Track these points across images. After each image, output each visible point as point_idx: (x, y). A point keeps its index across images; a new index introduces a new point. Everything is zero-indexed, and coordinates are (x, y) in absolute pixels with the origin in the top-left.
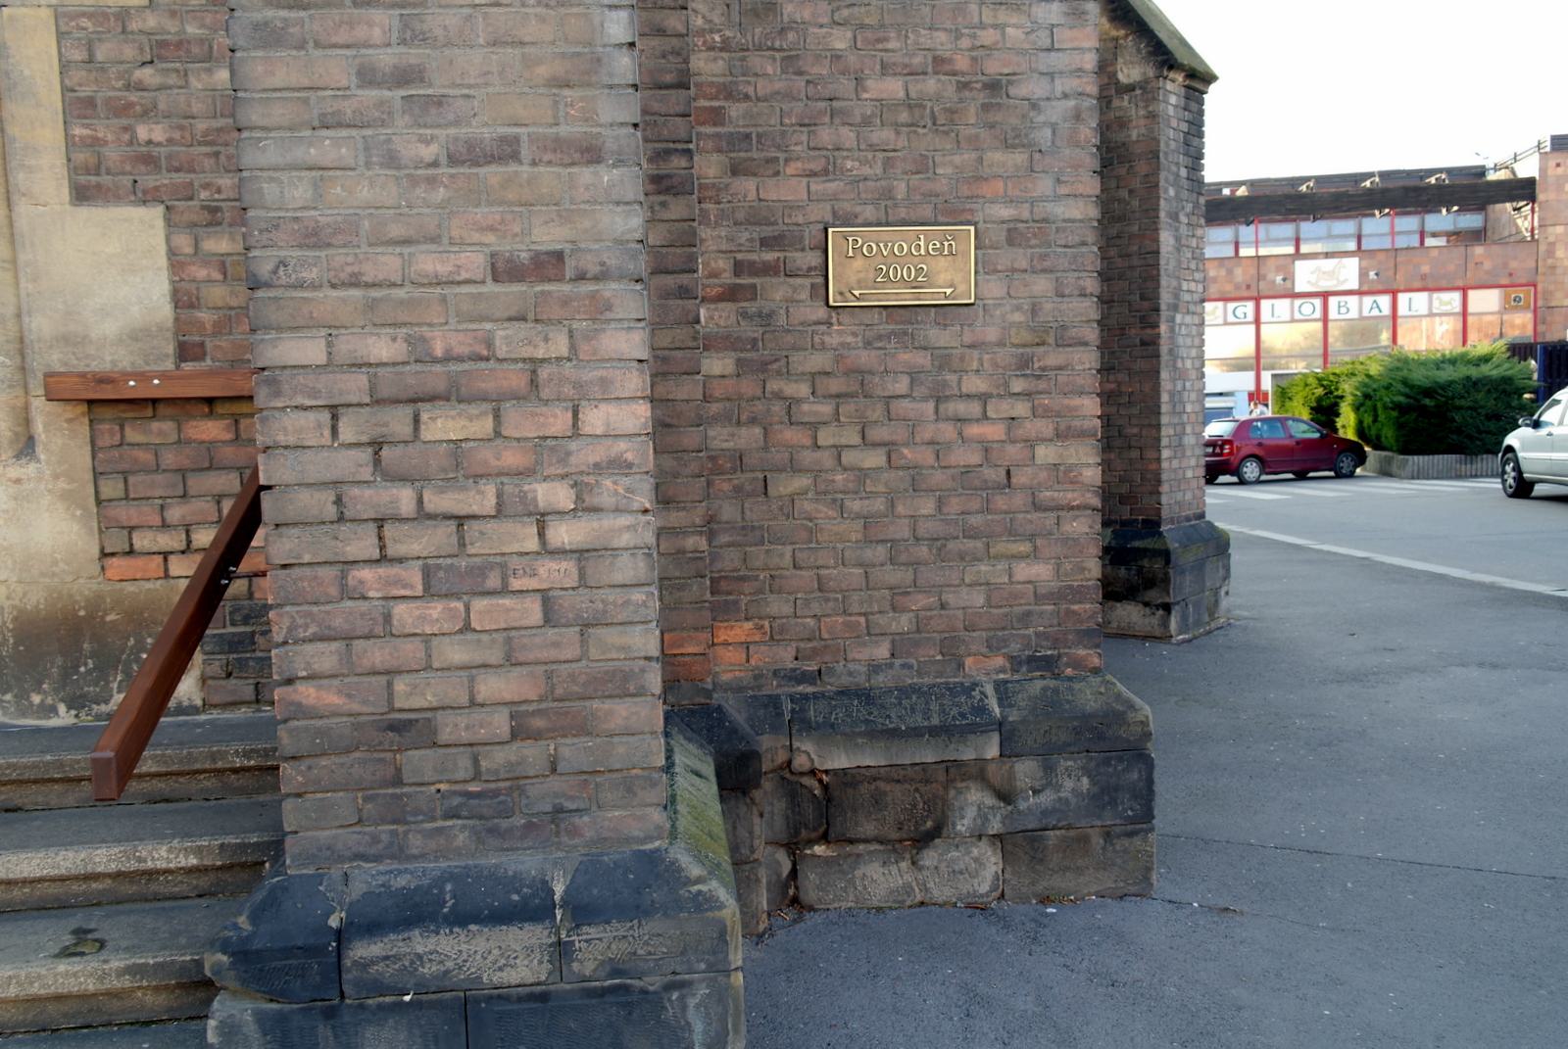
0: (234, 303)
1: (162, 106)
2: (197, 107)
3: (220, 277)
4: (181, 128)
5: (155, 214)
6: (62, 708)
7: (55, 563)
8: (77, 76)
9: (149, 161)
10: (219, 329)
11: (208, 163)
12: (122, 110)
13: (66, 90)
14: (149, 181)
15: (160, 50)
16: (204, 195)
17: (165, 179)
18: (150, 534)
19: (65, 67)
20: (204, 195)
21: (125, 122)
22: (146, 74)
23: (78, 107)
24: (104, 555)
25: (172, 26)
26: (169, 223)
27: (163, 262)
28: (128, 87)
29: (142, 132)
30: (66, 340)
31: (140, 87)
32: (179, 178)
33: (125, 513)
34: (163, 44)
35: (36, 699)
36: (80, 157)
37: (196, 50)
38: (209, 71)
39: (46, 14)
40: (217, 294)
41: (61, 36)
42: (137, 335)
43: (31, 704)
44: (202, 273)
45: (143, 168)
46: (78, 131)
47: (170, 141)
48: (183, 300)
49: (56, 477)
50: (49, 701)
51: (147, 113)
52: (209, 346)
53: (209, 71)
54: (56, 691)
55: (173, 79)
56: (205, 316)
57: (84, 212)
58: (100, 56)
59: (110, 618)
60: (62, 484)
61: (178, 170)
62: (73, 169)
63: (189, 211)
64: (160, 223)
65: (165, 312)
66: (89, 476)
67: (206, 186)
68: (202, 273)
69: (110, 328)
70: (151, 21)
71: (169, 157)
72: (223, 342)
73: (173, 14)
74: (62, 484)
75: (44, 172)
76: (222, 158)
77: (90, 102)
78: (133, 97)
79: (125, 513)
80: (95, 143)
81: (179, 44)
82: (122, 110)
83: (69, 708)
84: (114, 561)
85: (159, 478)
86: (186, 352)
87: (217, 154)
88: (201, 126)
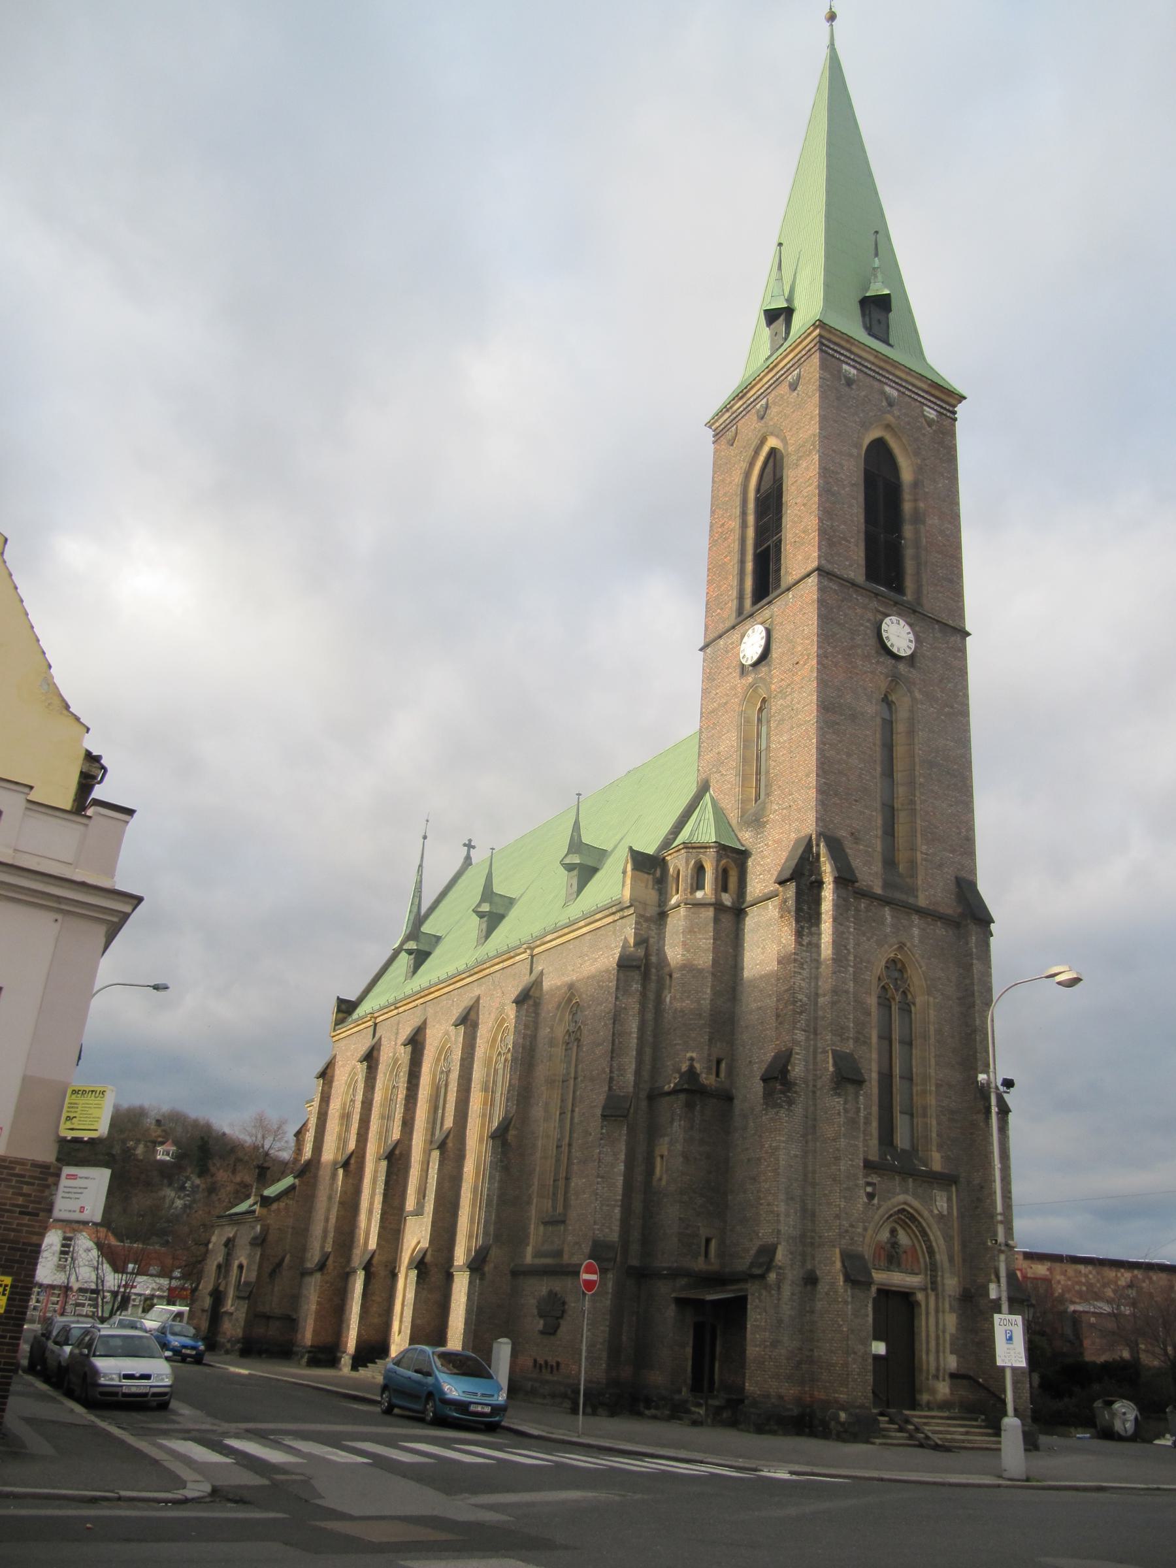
75: (948, 1350)
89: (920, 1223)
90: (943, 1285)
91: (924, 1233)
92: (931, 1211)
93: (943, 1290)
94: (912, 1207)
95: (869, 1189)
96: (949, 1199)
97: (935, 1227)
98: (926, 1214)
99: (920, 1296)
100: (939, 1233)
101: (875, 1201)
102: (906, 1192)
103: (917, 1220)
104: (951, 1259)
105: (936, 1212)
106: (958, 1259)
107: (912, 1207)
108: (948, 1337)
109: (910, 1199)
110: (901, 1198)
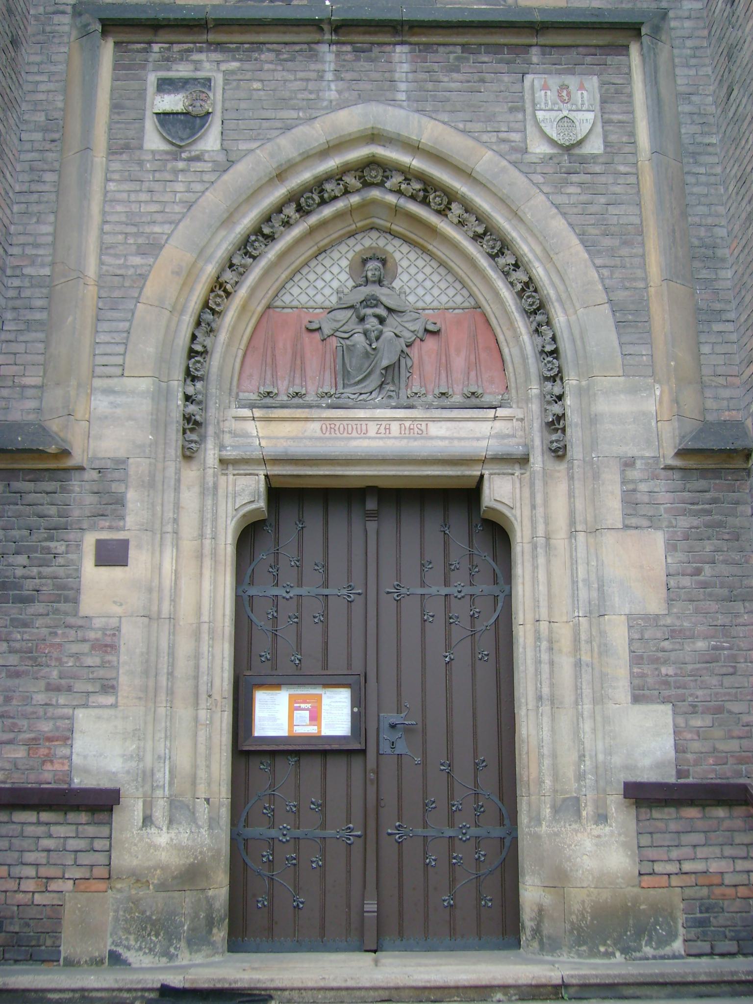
0: (703, 750)
1: (672, 658)
2: (688, 659)
3: (696, 737)
4: (681, 668)
5: (668, 708)
6: (618, 954)
7: (618, 877)
8: (636, 645)
9: (667, 683)
10: (697, 763)
11: (692, 684)
12: (655, 661)
13: (631, 651)
14: (666, 693)
15: (674, 634)
16: (690, 699)
17: (673, 692)
18: (662, 864)
19: (631, 640)
20: (690, 699)
21: (656, 666)
22: (666, 644)
23: (636, 659)
24: (640, 874)
25: (678, 623)
26: (675, 713)
27: (672, 731)
28: (657, 651)
29: (664, 670)
30: (627, 768)
31: (664, 650)
32: (680, 691)
33: (651, 853)
34: (673, 631)
35: (602, 949)
36: (636, 682)
37: (688, 633)
38: (693, 643)
39: (623, 618)
40: (696, 746)
41: (630, 627)
42: (659, 766)
43: (599, 951)
44: (689, 736)
45: (664, 687)
46: (635, 670)
47: (676, 675)
48: (679, 749)
49: (620, 835)
50: (610, 950)
51: (666, 662)
52: (691, 771)
53: (693, 643)
54: (615, 944)
55: (677, 647)
56: (689, 756)
57: (637, 707)
58: (646, 637)
59: (642, 907)
60: (622, 838)
61: (678, 688)
62: (634, 688)
63: (684, 706)
64: (670, 712)
65: (672, 754)
66: (635, 834)
67: (691, 695)
68: (689, 736)
69: (647, 762)
70: (669, 621)
71: (675, 682)
72: (698, 769)
73: (678, 618)
74: (622, 838)
75: (621, 690)
76: (698, 683)
77: (641, 657)
78: (660, 654)
79: (651, 853)
80: (643, 676)
81: (680, 631)
82: (655, 661)
83: (622, 953)
84: (646, 877)
85: (667, 836)
86: (680, 774)
87: (696, 680)
88: (690, 667)
89: (468, 208)
90: (593, 420)
91: (500, 247)
92: (517, 155)
93: (593, 444)
94: (415, 148)
95: (172, 102)
96: (614, 97)
97: (537, 205)
98: (485, 161)
99: (499, 492)
100: (559, 224)
101: (210, 141)
102: (383, 92)
103: (450, 197)
104: (630, 318)
105: (539, 148)
106: (662, 316)
107: (415, 148)
108: (619, 635)
109: (395, 117)
110: (351, 119)
